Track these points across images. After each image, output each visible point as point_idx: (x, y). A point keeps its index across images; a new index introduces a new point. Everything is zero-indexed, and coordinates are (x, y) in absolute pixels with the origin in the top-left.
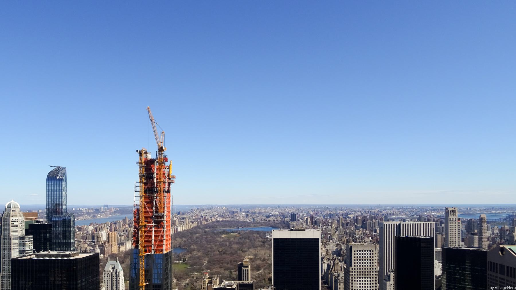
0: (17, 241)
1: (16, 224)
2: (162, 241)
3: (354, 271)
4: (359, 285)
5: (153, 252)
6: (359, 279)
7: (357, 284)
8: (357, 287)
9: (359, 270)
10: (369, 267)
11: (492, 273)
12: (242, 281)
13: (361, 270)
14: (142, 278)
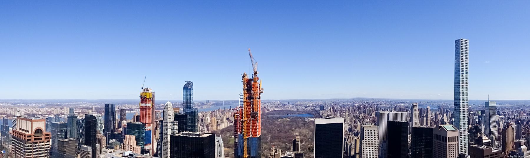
0: (171, 124)
1: (170, 114)
2: (256, 129)
5: (251, 136)
11: (435, 140)
14: (245, 152)
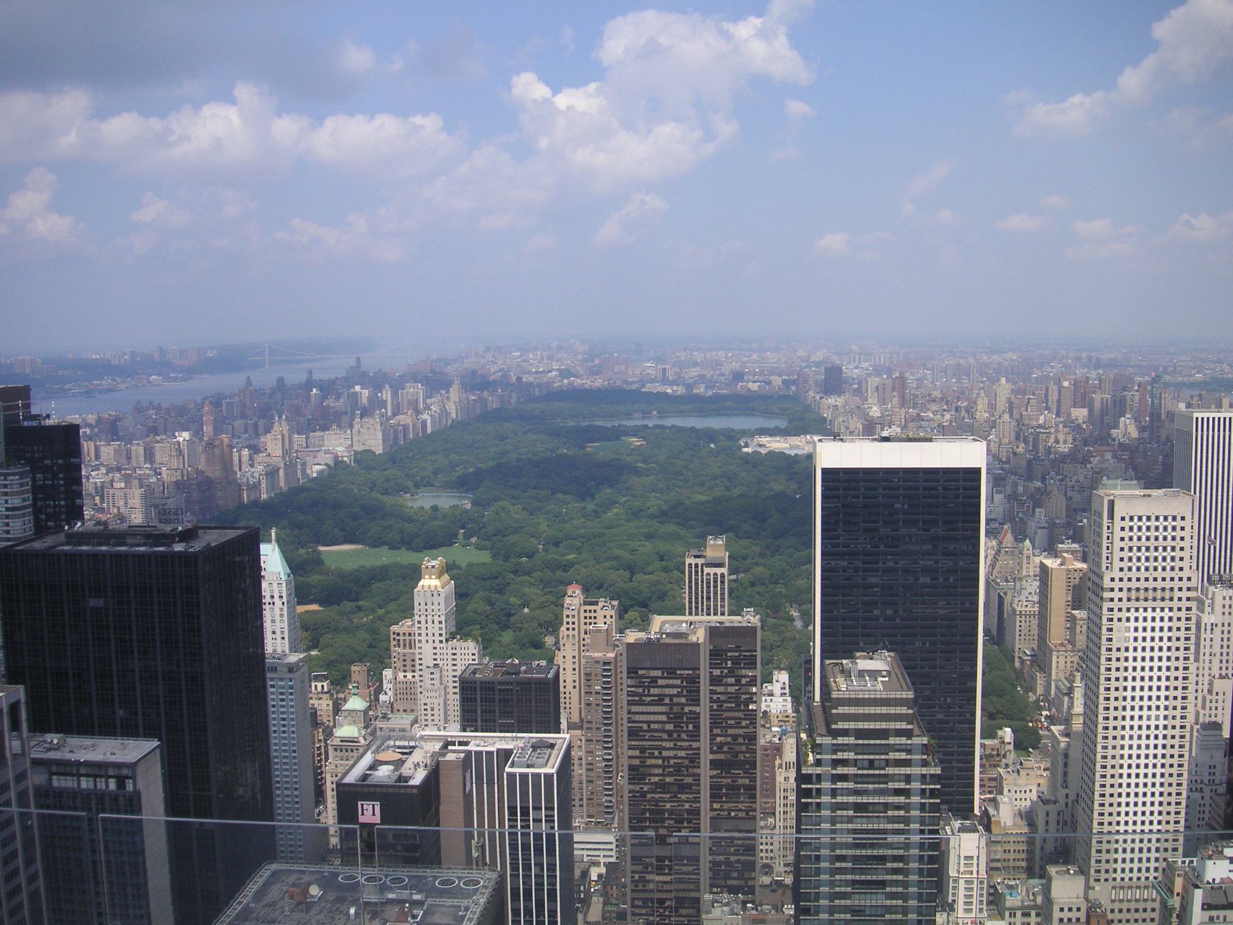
3: (1116, 585)
4: (1132, 634)
6: (1132, 615)
7: (1128, 629)
8: (1127, 639)
9: (1134, 584)
10: (1168, 574)
12: (719, 618)
13: (1142, 585)
